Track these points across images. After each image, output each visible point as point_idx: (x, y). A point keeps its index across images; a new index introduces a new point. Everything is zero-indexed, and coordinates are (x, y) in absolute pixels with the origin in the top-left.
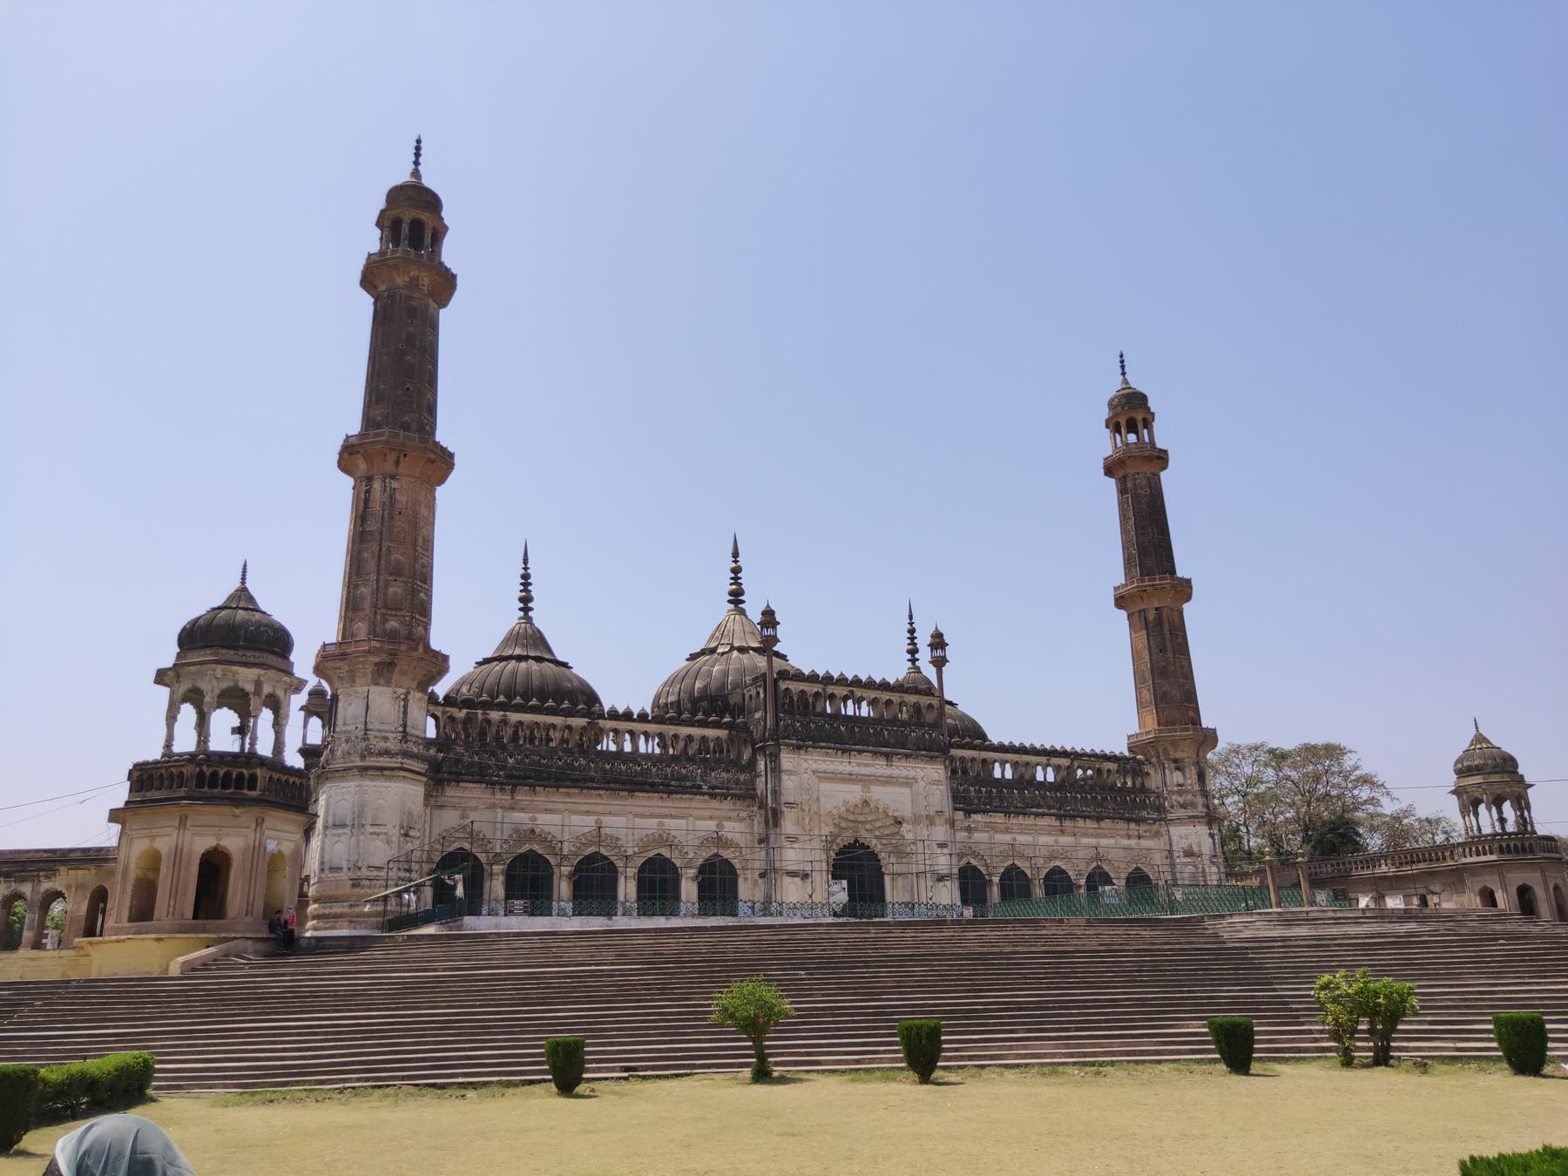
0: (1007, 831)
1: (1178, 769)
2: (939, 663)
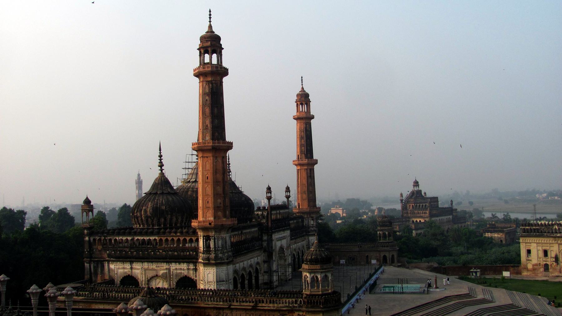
1: (313, 220)
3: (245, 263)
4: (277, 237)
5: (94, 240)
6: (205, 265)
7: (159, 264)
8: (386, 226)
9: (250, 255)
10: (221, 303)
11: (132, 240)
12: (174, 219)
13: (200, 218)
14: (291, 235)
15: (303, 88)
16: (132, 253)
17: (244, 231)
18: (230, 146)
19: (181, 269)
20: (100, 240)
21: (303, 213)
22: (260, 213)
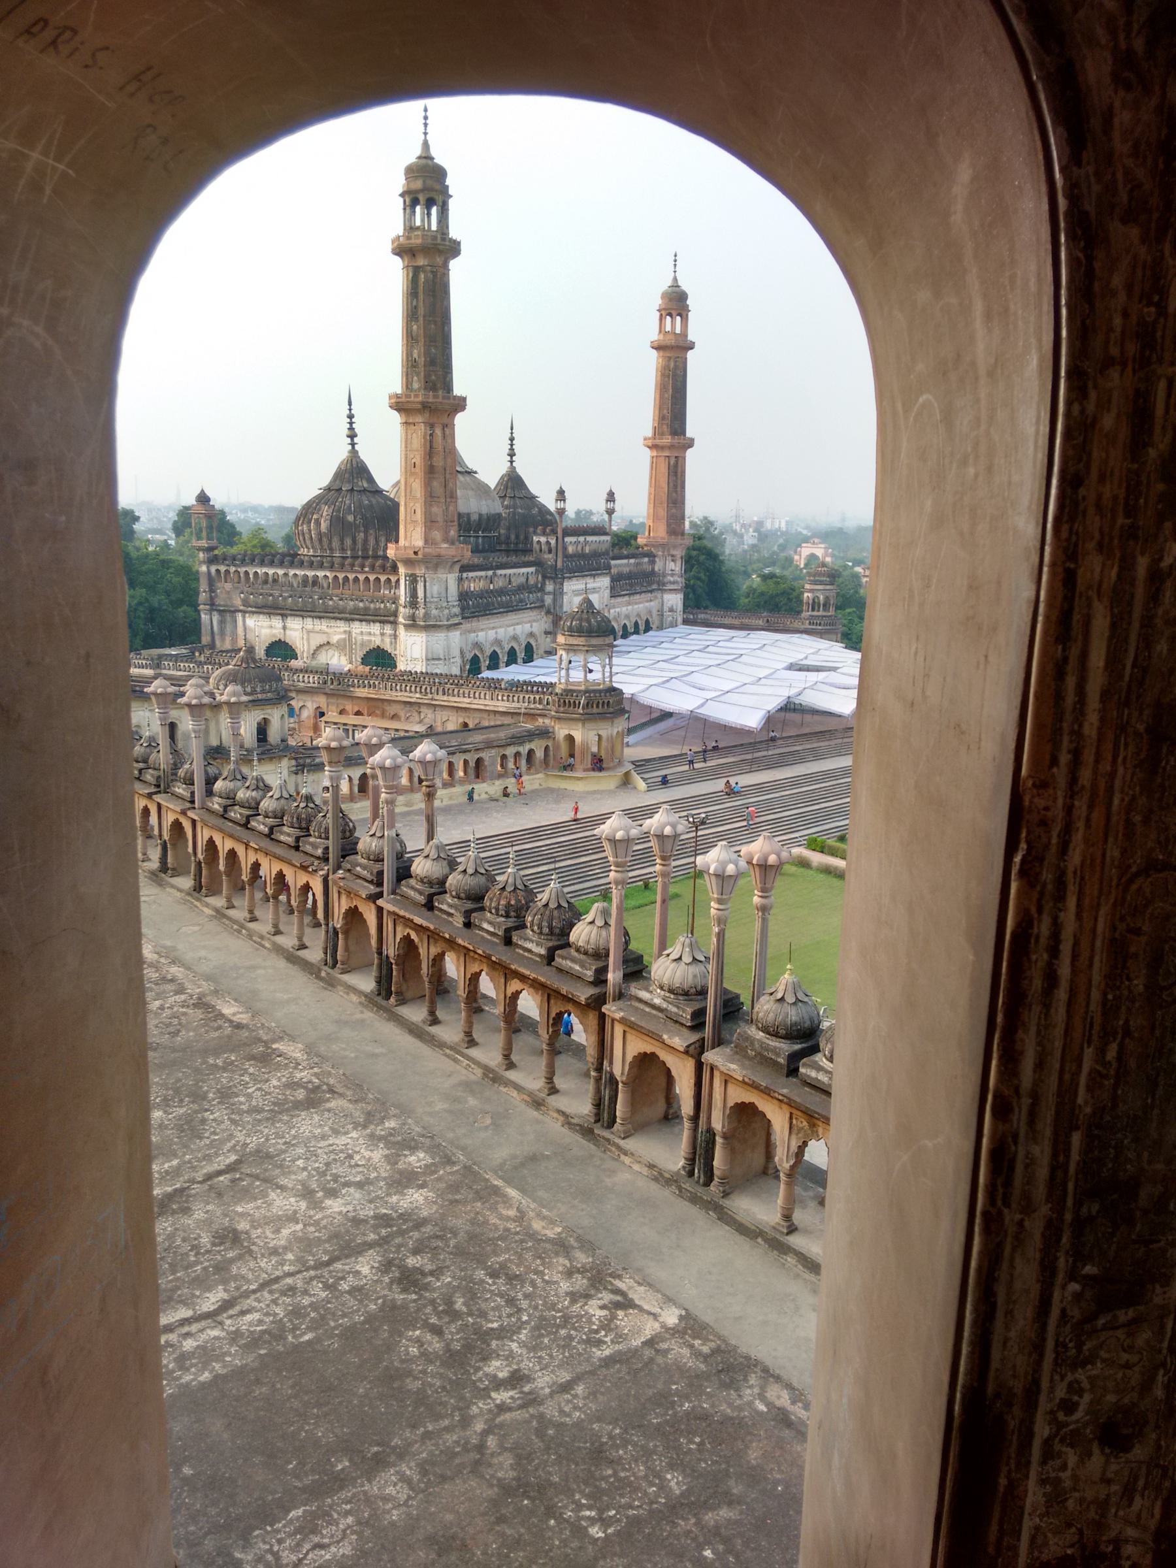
0: (614, 607)
2: (610, 512)
3: (501, 631)
4: (575, 588)
5: (218, 571)
6: (407, 627)
7: (333, 623)
8: (821, 583)
9: (512, 617)
10: (418, 695)
11: (286, 575)
12: (372, 542)
13: (402, 542)
14: (612, 588)
15: (675, 279)
16: (285, 599)
17: (499, 572)
18: (460, 404)
19: (370, 634)
20: (227, 572)
21: (653, 546)
22: (543, 539)
